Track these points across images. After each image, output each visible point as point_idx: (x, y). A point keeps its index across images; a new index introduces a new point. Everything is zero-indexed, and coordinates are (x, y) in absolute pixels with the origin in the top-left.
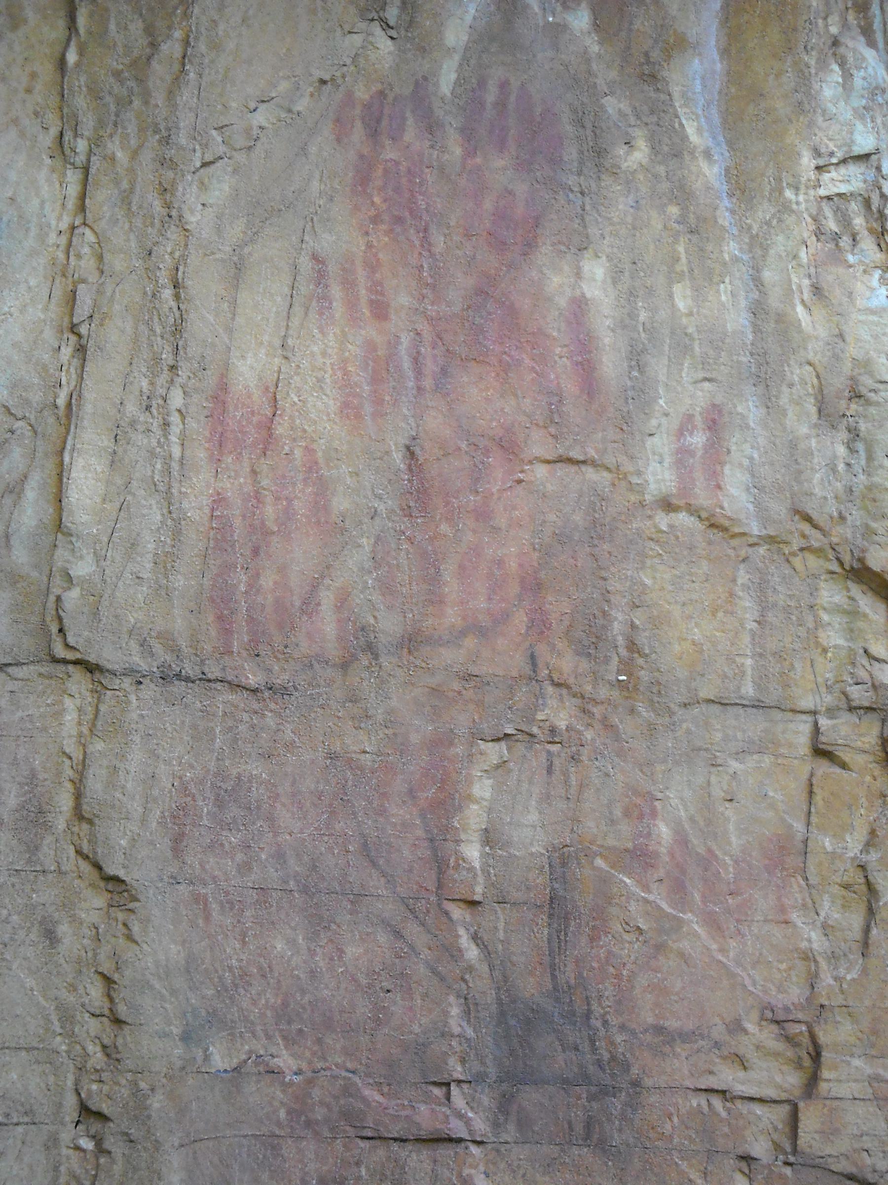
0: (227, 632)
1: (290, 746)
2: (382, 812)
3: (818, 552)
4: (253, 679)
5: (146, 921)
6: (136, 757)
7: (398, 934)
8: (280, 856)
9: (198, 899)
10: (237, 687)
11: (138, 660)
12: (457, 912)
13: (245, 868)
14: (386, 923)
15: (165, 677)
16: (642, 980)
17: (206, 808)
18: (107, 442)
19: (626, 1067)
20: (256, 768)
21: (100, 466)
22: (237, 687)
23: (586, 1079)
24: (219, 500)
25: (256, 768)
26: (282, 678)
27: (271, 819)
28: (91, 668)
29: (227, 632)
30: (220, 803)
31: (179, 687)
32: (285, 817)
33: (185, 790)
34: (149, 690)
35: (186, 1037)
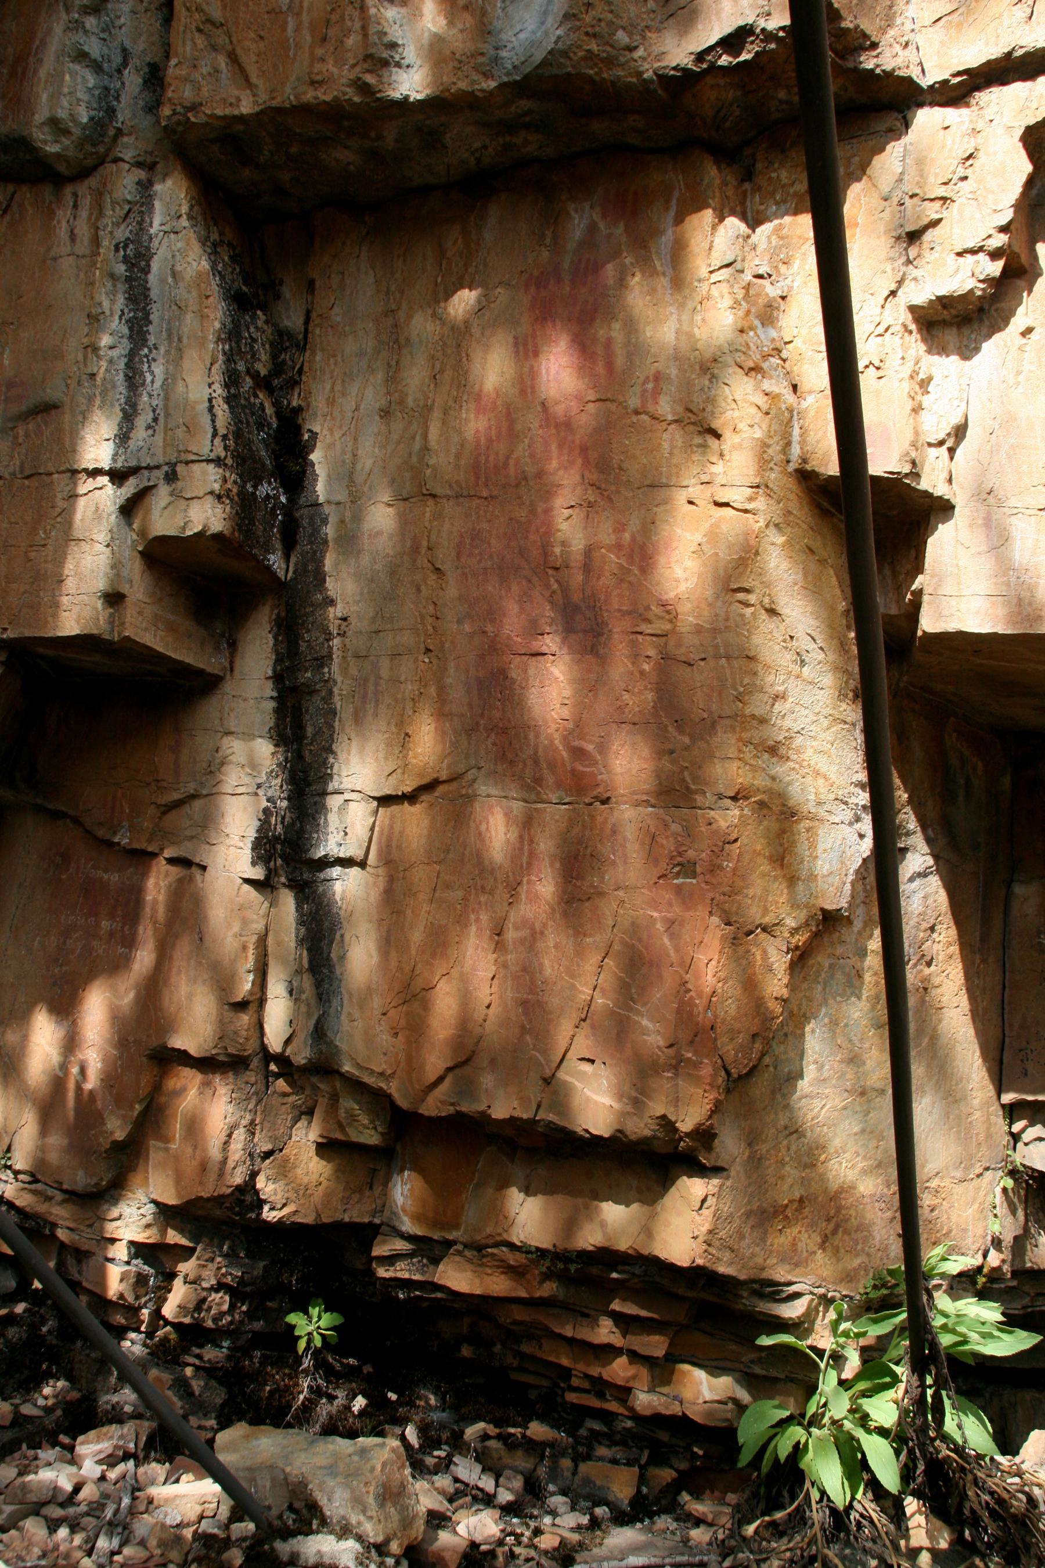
0: (478, 478)
1: (497, 517)
2: (527, 538)
3: (694, 424)
4: (485, 494)
5: (447, 583)
6: (447, 526)
7: (530, 581)
8: (491, 557)
9: (464, 574)
10: (480, 497)
11: (449, 493)
12: (550, 572)
13: (480, 562)
14: (526, 578)
15: (458, 496)
16: (615, 593)
17: (468, 541)
18: (441, 416)
19: (607, 625)
20: (485, 526)
21: (439, 424)
22: (480, 497)
23: (592, 630)
24: (477, 431)
25: (485, 526)
26: (495, 493)
27: (489, 544)
28: (434, 496)
29: (478, 478)
30: (473, 540)
31: (461, 500)
32: (494, 542)
33: (461, 536)
34: (451, 503)
35: (458, 622)
